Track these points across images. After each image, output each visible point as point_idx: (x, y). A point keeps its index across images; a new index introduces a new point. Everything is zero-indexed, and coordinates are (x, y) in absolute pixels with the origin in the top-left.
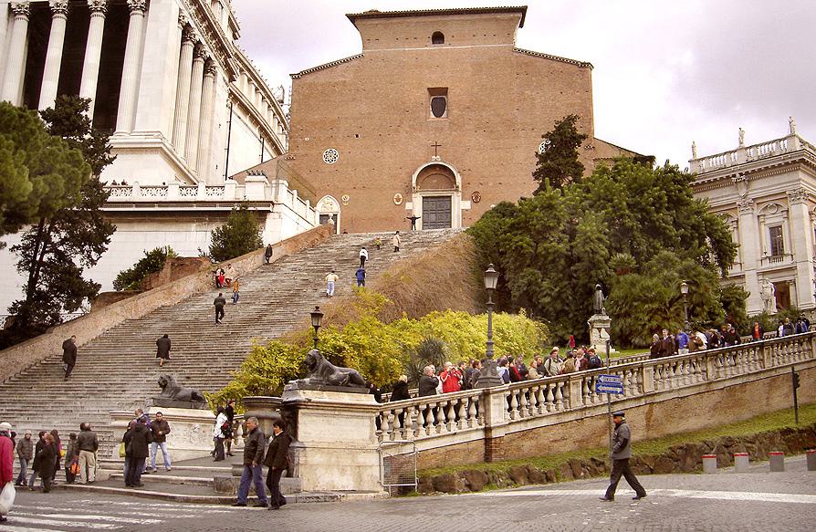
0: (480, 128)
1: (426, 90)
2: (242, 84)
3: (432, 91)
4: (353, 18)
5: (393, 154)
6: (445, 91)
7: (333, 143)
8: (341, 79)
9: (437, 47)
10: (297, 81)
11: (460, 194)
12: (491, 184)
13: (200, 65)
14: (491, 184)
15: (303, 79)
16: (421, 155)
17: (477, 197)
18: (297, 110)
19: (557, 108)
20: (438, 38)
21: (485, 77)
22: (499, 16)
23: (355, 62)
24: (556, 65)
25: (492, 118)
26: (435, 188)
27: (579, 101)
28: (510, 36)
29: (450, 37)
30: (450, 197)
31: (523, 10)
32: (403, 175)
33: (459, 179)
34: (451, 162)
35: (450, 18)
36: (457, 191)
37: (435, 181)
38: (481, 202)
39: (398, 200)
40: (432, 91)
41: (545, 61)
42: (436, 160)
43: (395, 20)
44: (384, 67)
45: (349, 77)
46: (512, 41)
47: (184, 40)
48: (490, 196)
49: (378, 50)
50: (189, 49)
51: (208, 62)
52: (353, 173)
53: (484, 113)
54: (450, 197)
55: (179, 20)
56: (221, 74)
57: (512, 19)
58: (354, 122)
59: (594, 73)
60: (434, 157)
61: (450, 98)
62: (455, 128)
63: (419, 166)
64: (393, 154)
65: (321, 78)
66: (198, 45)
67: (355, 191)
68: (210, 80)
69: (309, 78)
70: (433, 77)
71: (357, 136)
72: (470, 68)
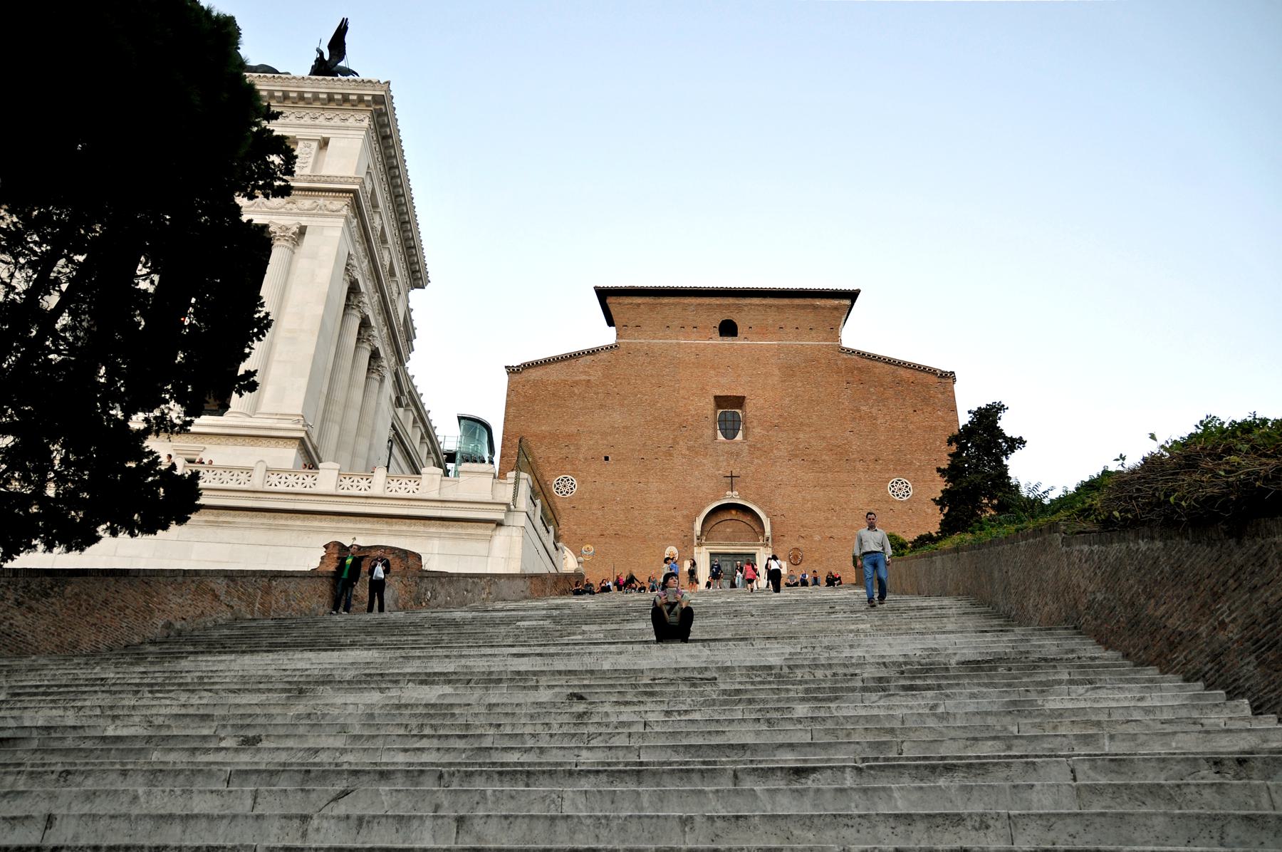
0: (796, 456)
1: (712, 400)
2: (407, 417)
5: (663, 487)
6: (739, 402)
7: (568, 467)
8: (584, 377)
9: (728, 341)
10: (517, 377)
12: (817, 538)
13: (365, 356)
14: (817, 538)
15: (526, 374)
16: (706, 490)
17: (796, 557)
18: (515, 417)
19: (910, 432)
20: (728, 329)
21: (799, 384)
22: (818, 302)
23: (604, 355)
24: (902, 372)
25: (813, 442)
26: (730, 539)
27: (943, 424)
28: (834, 331)
29: (746, 329)
30: (754, 555)
31: (852, 295)
32: (680, 519)
34: (755, 503)
37: (728, 530)
38: (803, 564)
40: (721, 401)
41: (886, 366)
42: (733, 497)
43: (666, 300)
44: (649, 363)
45: (596, 375)
46: (837, 337)
47: (347, 306)
48: (817, 555)
49: (638, 341)
50: (355, 323)
51: (375, 355)
52: (599, 513)
53: (801, 436)
54: (754, 555)
55: (346, 268)
56: (389, 381)
57: (836, 308)
58: (602, 439)
59: (958, 388)
62: (758, 453)
63: (704, 507)
64: (663, 487)
65: (554, 373)
66: (365, 324)
67: (602, 540)
68: (375, 384)
69: (534, 374)
70: (723, 381)
71: (607, 459)
72: (777, 372)
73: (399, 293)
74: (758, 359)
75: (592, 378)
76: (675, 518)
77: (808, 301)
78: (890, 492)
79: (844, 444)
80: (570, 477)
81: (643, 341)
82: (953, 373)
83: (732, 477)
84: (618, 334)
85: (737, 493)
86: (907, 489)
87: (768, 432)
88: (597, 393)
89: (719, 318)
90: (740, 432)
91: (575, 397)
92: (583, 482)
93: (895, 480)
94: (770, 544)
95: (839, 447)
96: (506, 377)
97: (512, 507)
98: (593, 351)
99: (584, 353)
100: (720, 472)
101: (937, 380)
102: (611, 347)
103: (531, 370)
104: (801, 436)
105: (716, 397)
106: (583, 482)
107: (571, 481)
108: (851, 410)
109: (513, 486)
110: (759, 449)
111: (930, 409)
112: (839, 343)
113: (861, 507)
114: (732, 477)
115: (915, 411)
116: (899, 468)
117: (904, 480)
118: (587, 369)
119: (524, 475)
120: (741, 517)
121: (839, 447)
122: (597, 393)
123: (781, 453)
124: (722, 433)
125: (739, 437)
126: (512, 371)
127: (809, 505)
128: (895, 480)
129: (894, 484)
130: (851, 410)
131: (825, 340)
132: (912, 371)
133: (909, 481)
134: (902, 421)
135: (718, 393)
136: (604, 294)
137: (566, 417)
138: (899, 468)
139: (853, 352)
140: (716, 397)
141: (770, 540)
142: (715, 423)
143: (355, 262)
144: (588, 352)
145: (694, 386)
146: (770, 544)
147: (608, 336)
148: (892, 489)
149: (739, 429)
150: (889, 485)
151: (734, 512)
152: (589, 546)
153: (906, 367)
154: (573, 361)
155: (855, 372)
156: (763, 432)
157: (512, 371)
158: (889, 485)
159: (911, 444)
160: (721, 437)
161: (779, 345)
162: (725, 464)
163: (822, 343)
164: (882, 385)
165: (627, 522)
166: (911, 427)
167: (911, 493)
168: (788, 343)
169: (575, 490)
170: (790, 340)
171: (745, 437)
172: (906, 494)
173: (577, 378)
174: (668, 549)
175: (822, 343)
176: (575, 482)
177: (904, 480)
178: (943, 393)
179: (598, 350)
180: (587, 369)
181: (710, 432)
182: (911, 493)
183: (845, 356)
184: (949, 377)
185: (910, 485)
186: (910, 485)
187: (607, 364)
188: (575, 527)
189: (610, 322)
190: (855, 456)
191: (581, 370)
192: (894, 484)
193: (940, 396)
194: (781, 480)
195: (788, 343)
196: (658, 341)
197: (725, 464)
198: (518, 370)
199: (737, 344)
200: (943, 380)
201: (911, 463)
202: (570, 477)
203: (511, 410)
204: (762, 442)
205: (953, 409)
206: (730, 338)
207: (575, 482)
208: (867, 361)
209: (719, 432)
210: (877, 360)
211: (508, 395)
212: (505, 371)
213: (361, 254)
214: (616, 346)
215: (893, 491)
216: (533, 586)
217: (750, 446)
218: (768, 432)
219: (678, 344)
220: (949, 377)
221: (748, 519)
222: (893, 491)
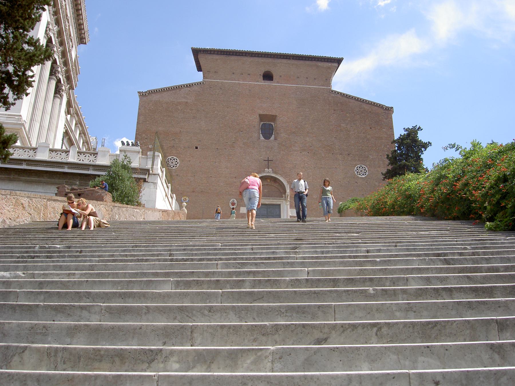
1: (258, 116)
3: (262, 117)
4: (197, 52)
6: (273, 118)
8: (184, 100)
9: (267, 83)
10: (145, 98)
11: (288, 203)
20: (268, 76)
21: (307, 110)
23: (196, 88)
27: (386, 136)
28: (328, 80)
30: (280, 205)
31: (339, 61)
33: (288, 191)
34: (281, 175)
35: (280, 61)
36: (286, 199)
37: (265, 190)
39: (233, 204)
40: (262, 117)
41: (357, 103)
43: (233, 58)
46: (329, 85)
53: (308, 139)
54: (280, 205)
55: (46, 31)
57: (329, 68)
59: (394, 116)
60: (266, 169)
61: (279, 124)
65: (166, 97)
69: (155, 97)
71: (197, 148)
73: (72, 47)
74: (285, 94)
75: (189, 101)
76: (235, 183)
77: (314, 63)
78: (356, 173)
79: (331, 145)
80: (175, 158)
81: (219, 81)
82: (393, 108)
83: (268, 161)
84: (204, 76)
85: (271, 170)
86: (365, 171)
87: (289, 136)
88: (192, 110)
89: (263, 70)
90: (273, 136)
91: (179, 112)
92: (183, 161)
93: (359, 166)
94: (289, 199)
95: (328, 146)
96: (138, 99)
97: (151, 172)
98: (190, 85)
99: (184, 86)
100: (262, 158)
101: (383, 111)
102: (200, 83)
103: (153, 95)
104: (308, 139)
105: (260, 115)
106: (183, 161)
107: (176, 160)
108: (336, 126)
109: (152, 159)
110: (283, 145)
111: (379, 127)
112: (330, 88)
113: (340, 180)
114: (268, 161)
115: (371, 128)
116: (361, 159)
117: (363, 166)
118: (186, 96)
119: (157, 153)
120: (273, 183)
121: (328, 146)
122: (192, 110)
123: (296, 149)
124: (263, 136)
125: (272, 138)
126: (142, 95)
127: (311, 178)
128: (359, 166)
129: (358, 168)
130: (336, 126)
131: (322, 86)
132: (370, 106)
133: (367, 167)
134: (364, 133)
135: (261, 113)
136: (197, 52)
137: (173, 123)
138: (361, 159)
139: (338, 93)
140: (260, 115)
141: (289, 197)
142: (259, 130)
143: (51, 27)
144: (187, 86)
145: (248, 108)
146: (289, 199)
147: (199, 77)
148: (357, 171)
149: (273, 134)
150: (356, 169)
151: (269, 181)
152: (185, 197)
153: (367, 103)
154: (178, 90)
155: (339, 104)
156: (286, 136)
157: (142, 95)
158: (356, 169)
159: (368, 146)
160: (262, 138)
161: (296, 87)
162: (264, 153)
163: (320, 87)
164: (354, 112)
165: (208, 184)
166: (368, 137)
167: (367, 173)
168: (301, 86)
169: (178, 165)
170: (303, 85)
171: (275, 139)
172: (364, 174)
173: (180, 101)
174: (232, 200)
175: (320, 87)
176: (178, 161)
177: (363, 166)
178: (386, 119)
179: (192, 85)
180: (186, 96)
181: (256, 135)
182: (367, 173)
183: (333, 95)
184: (389, 110)
185: (367, 169)
186: (367, 169)
187: (198, 93)
188: (178, 186)
189: (199, 69)
190: (337, 151)
191: (182, 96)
192: (358, 168)
193: (384, 120)
194: (296, 164)
195: (301, 86)
196: (227, 81)
197: (264, 153)
198: (145, 94)
199: (273, 85)
200: (387, 112)
201: (368, 157)
202: (175, 158)
203: (141, 118)
204: (286, 141)
205: (391, 128)
206: (269, 82)
207: (178, 161)
208: (345, 99)
209: (261, 135)
210: (350, 98)
211: (139, 109)
212: (137, 94)
213: (54, 22)
214: (203, 83)
215: (358, 172)
216: (163, 217)
217: (278, 143)
218: (289, 136)
219: (239, 84)
220: (389, 110)
221: (276, 185)
222: (358, 172)
